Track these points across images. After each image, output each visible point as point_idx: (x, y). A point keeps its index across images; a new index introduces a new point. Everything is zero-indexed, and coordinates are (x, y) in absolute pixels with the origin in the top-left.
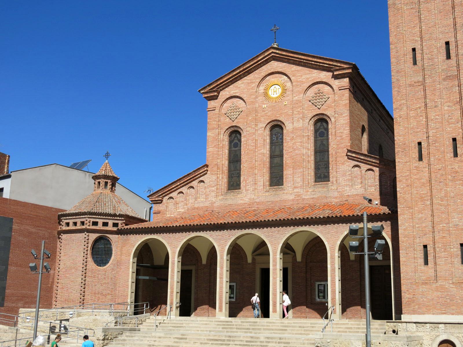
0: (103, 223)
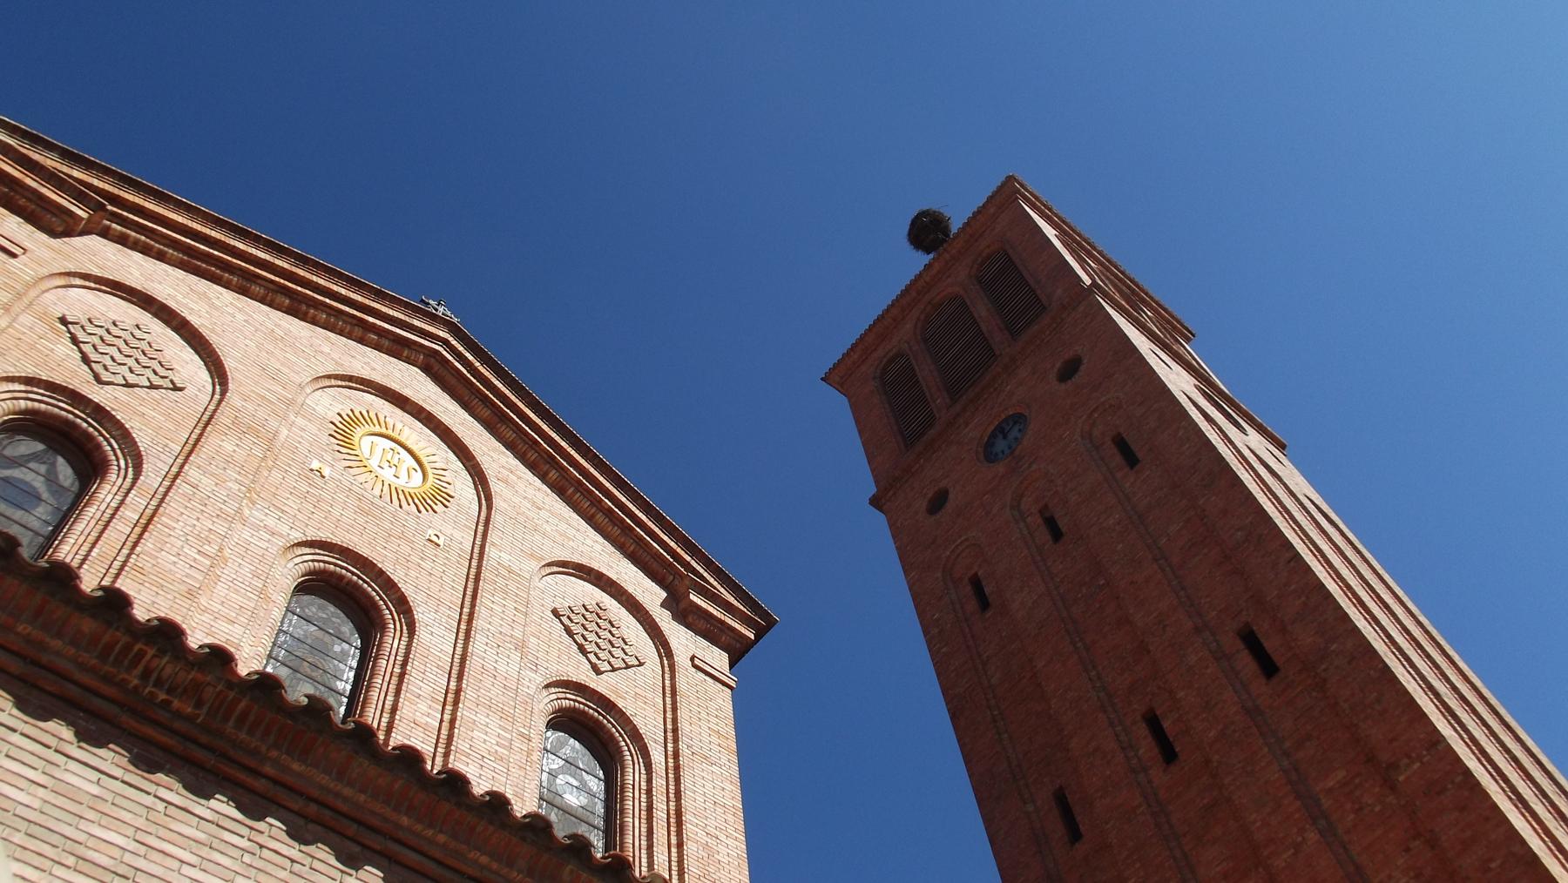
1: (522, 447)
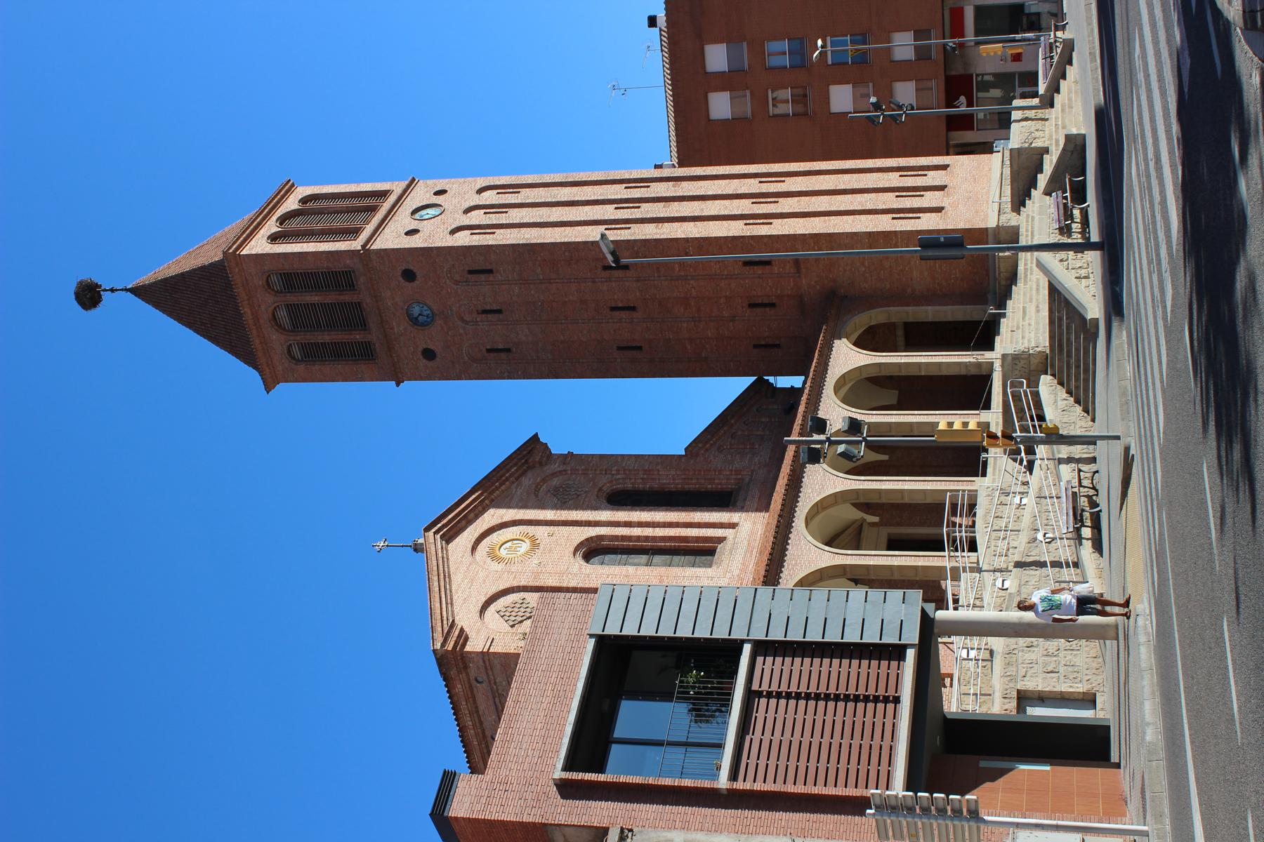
1: (477, 512)
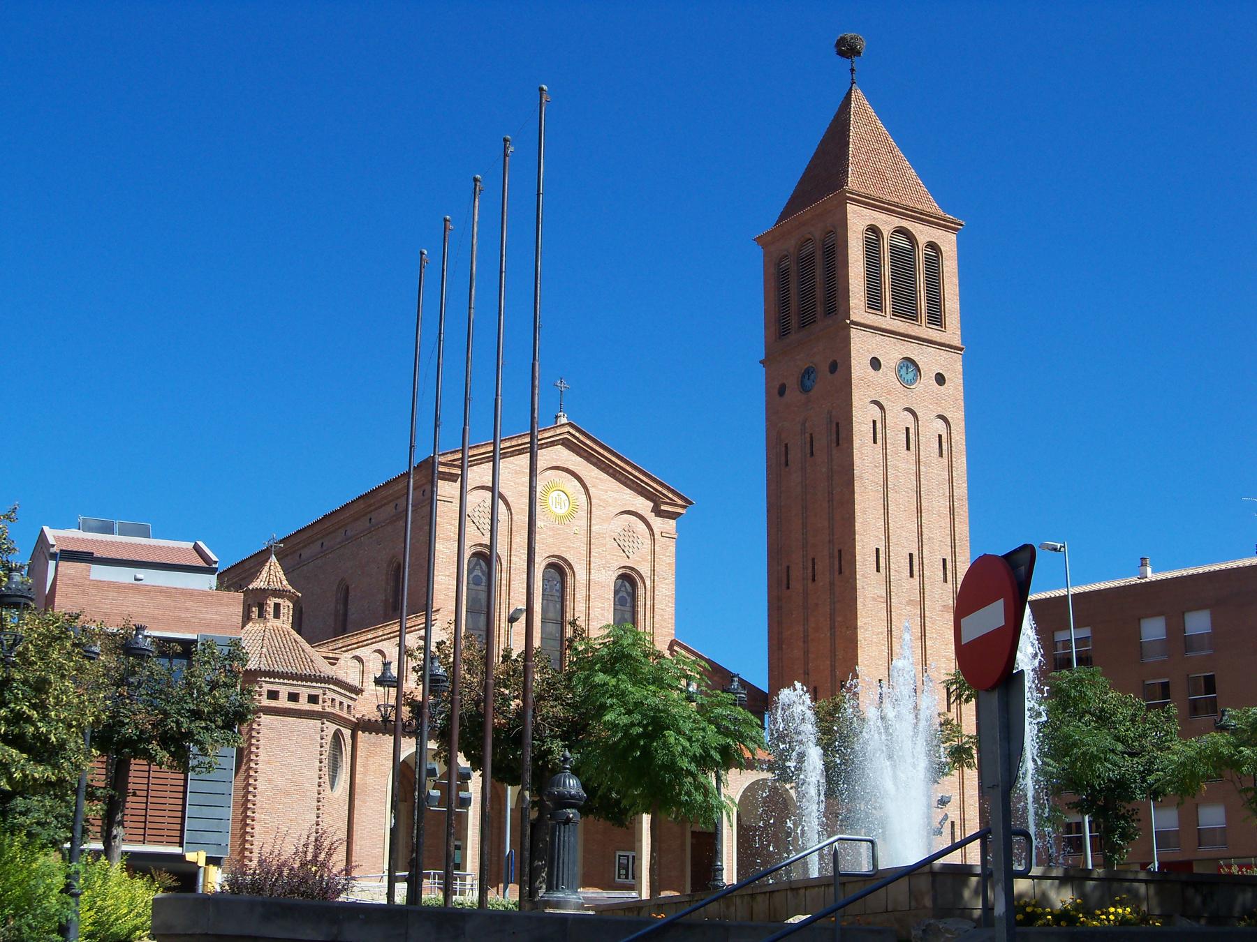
0: (290, 694)
1: (599, 464)
